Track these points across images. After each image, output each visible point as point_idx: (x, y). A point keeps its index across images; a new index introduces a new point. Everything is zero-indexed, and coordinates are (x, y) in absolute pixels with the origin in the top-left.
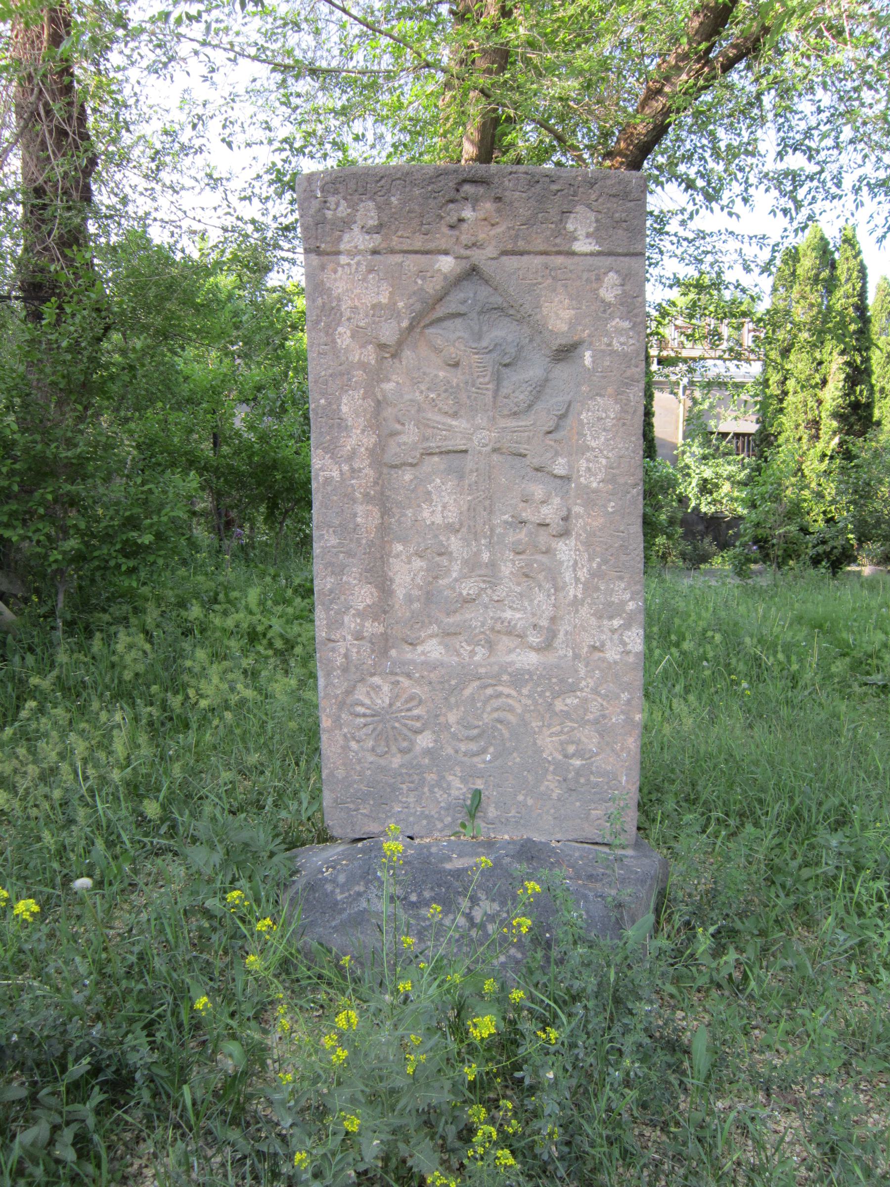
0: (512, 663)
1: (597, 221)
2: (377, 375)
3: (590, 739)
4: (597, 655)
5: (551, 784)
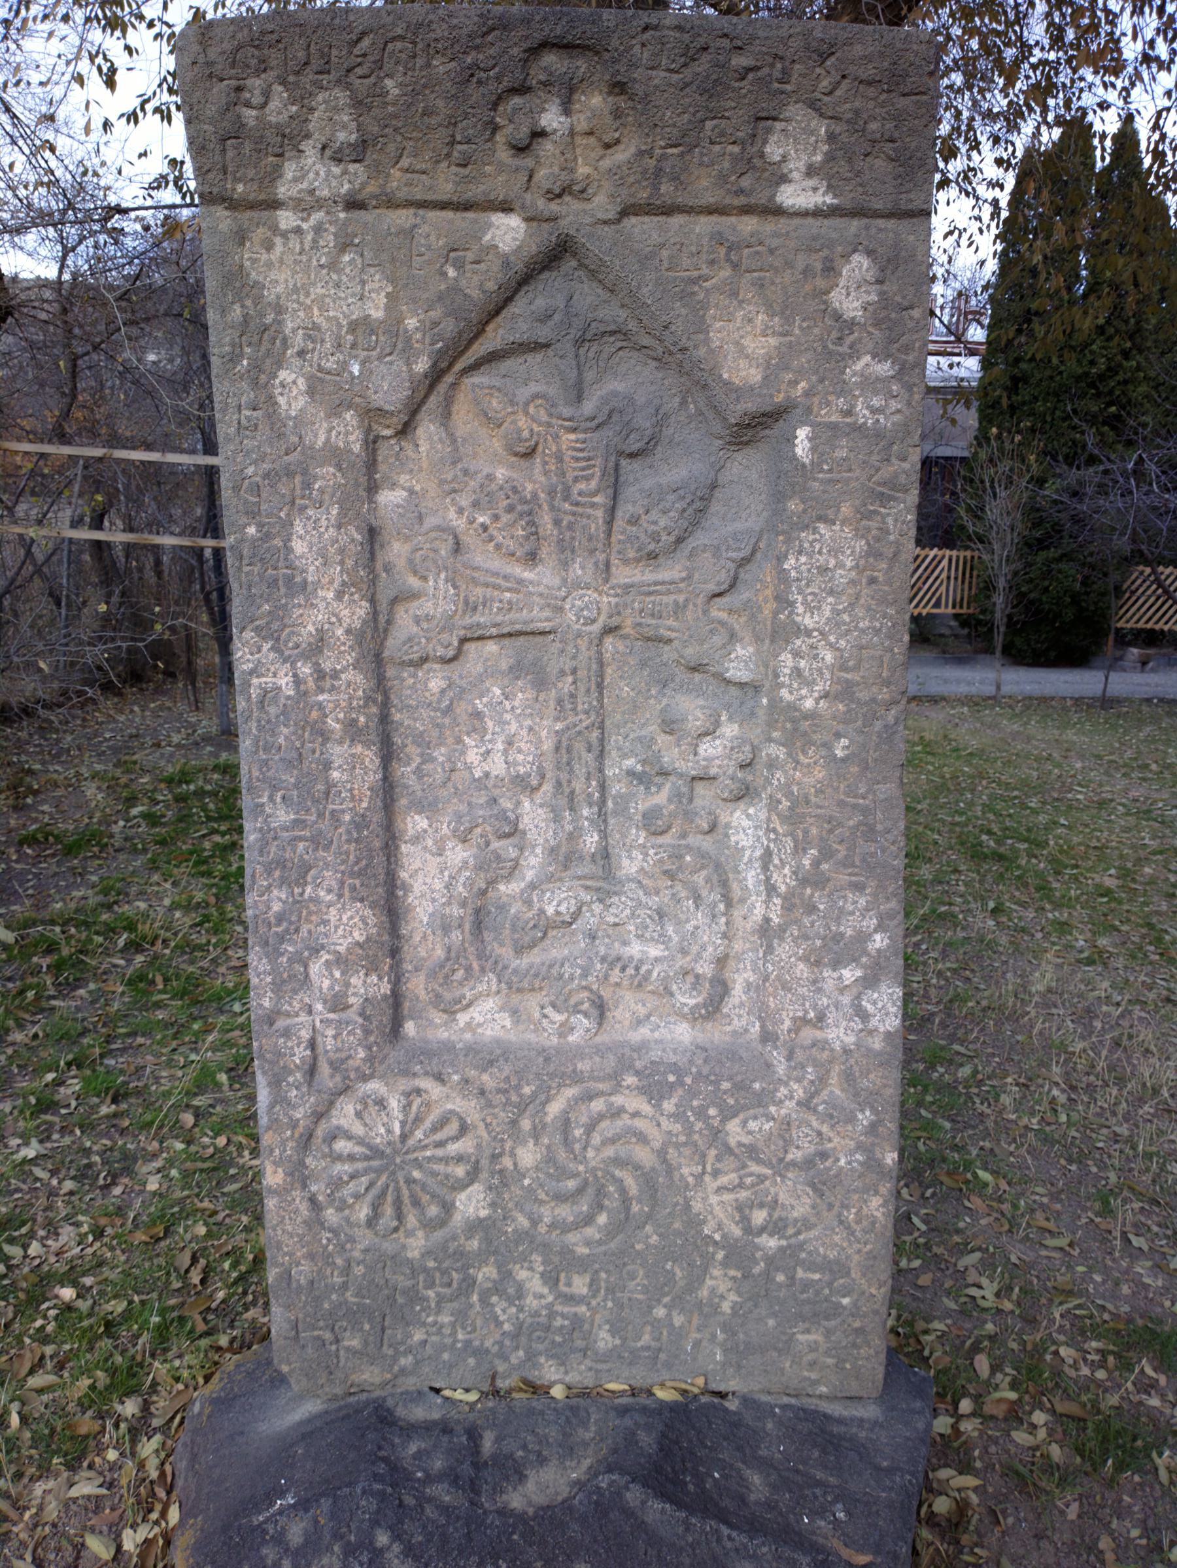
0: (642, 1047)
1: (831, 137)
3: (795, 1199)
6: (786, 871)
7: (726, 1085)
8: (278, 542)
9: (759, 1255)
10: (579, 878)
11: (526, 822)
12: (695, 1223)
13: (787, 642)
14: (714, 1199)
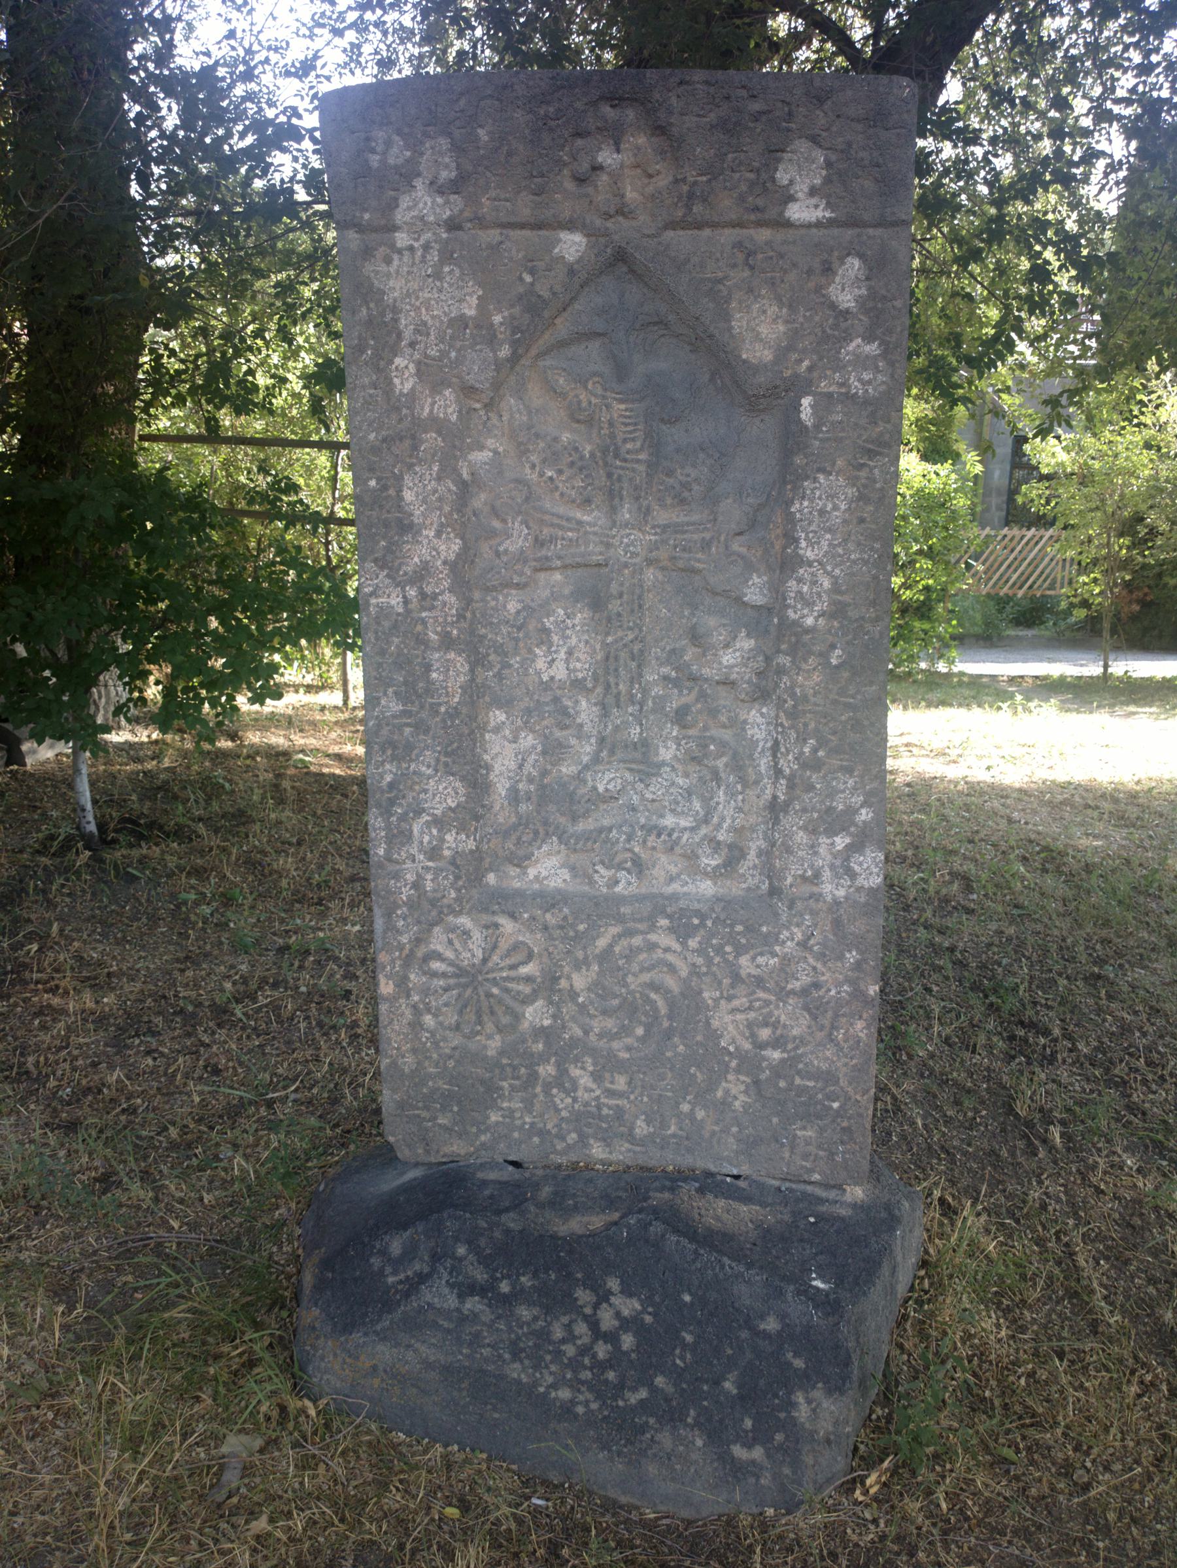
0: (675, 897)
1: (828, 164)
2: (457, 439)
3: (795, 1021)
4: (807, 889)
5: (735, 1088)
6: (790, 757)
7: (739, 928)
8: (392, 492)
9: (764, 1064)
10: (624, 762)
11: (583, 718)
12: (714, 1036)
13: (793, 571)
14: (728, 1018)
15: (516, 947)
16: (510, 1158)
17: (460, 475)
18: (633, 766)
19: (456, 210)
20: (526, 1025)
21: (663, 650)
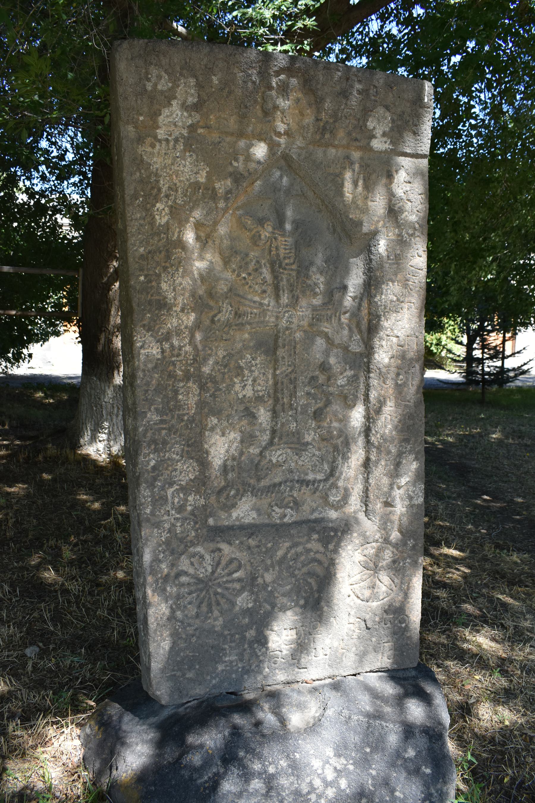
0: (317, 521)
6: (378, 436)
15: (231, 561)
16: (230, 691)
17: (194, 275)
18: (292, 446)
19: (195, 121)
20: (237, 608)
21: (306, 377)
